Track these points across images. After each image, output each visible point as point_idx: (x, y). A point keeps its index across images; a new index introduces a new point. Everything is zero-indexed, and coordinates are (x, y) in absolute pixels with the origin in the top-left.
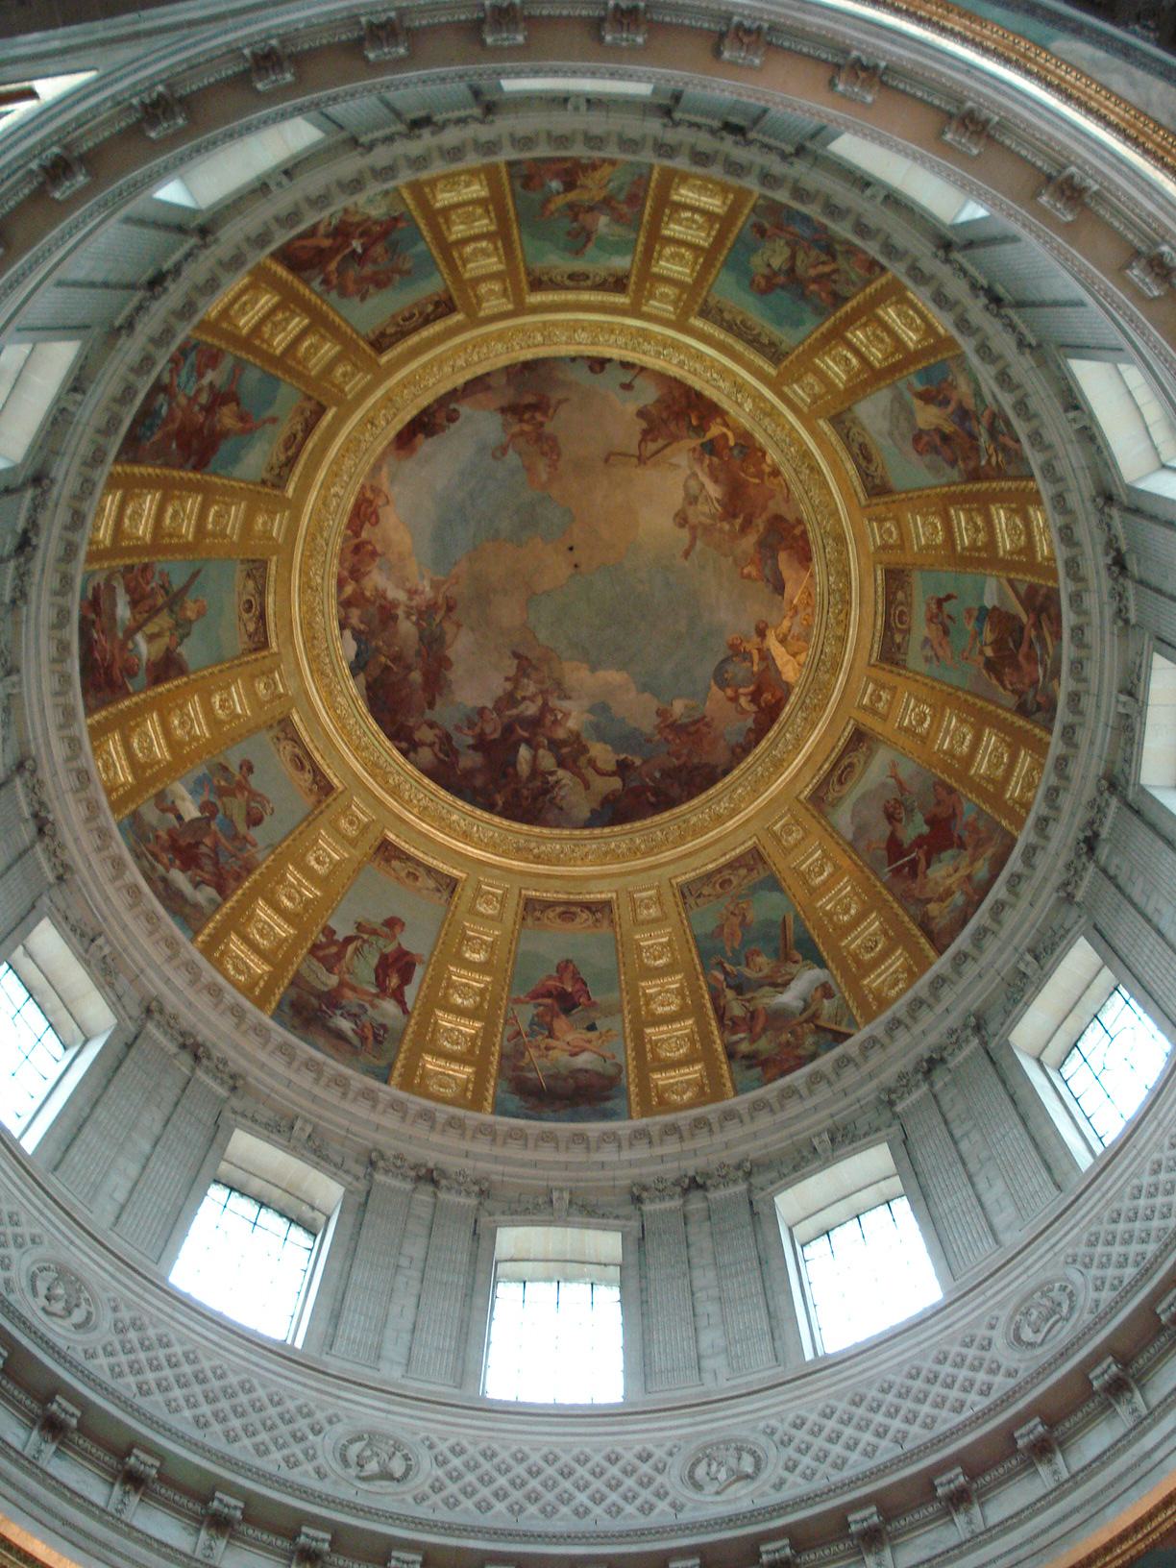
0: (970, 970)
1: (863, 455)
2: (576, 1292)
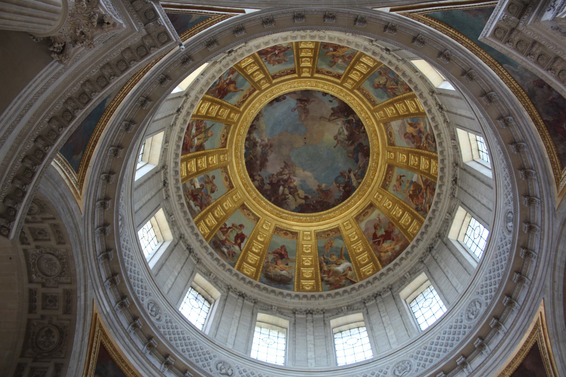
0: (391, 273)
1: (390, 135)
2: (274, 333)
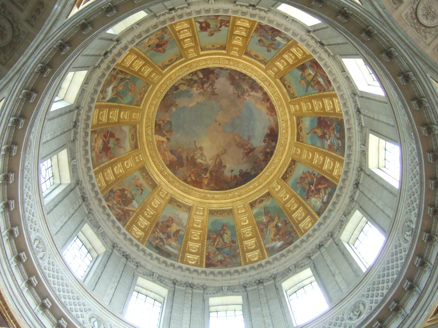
1: (180, 205)
